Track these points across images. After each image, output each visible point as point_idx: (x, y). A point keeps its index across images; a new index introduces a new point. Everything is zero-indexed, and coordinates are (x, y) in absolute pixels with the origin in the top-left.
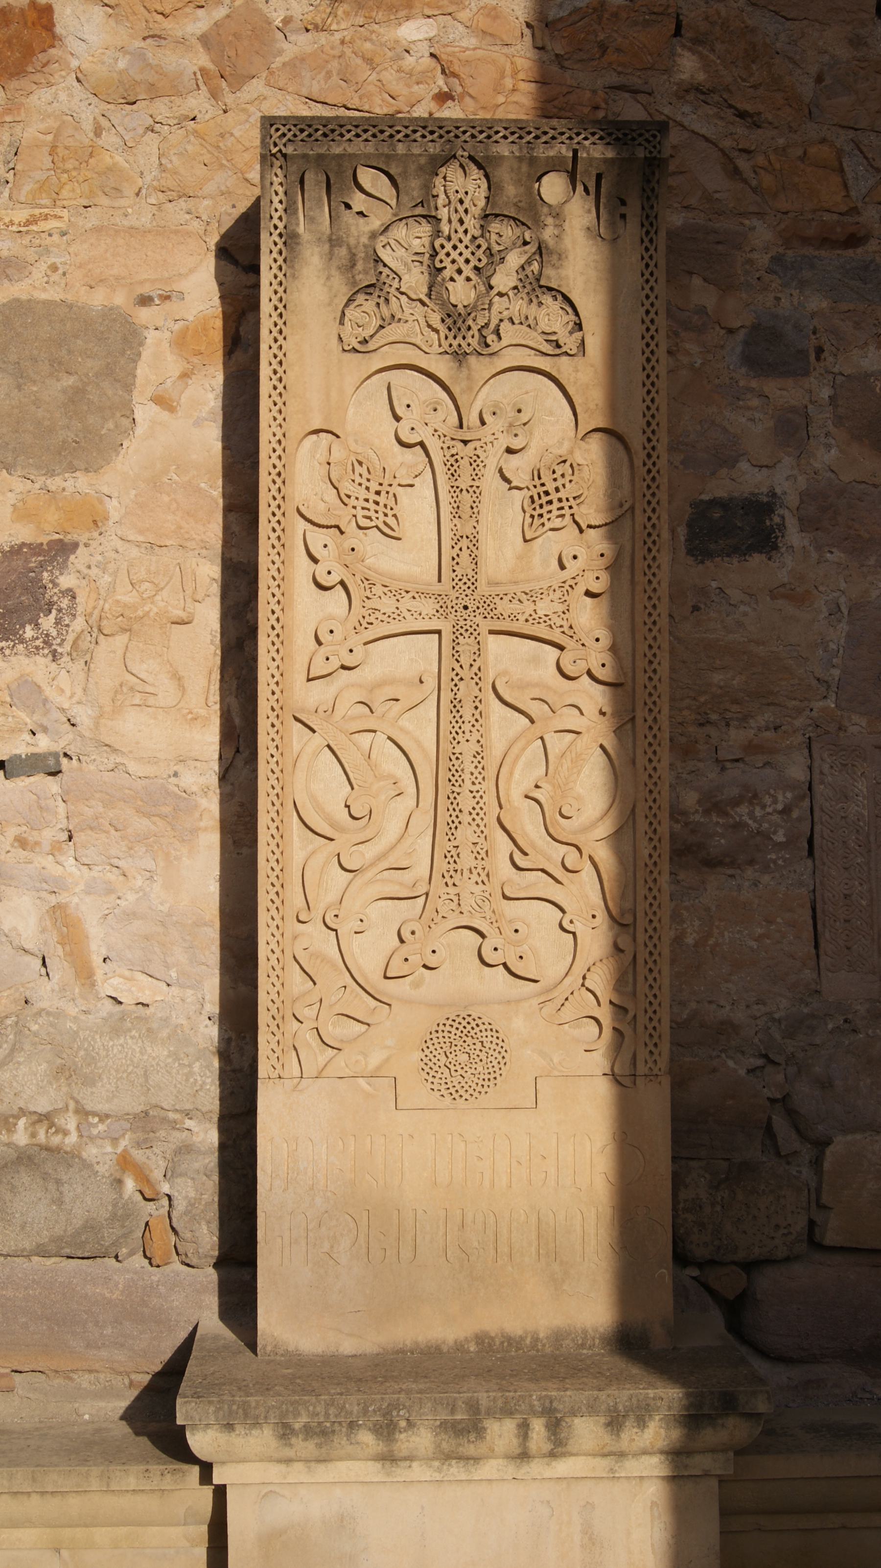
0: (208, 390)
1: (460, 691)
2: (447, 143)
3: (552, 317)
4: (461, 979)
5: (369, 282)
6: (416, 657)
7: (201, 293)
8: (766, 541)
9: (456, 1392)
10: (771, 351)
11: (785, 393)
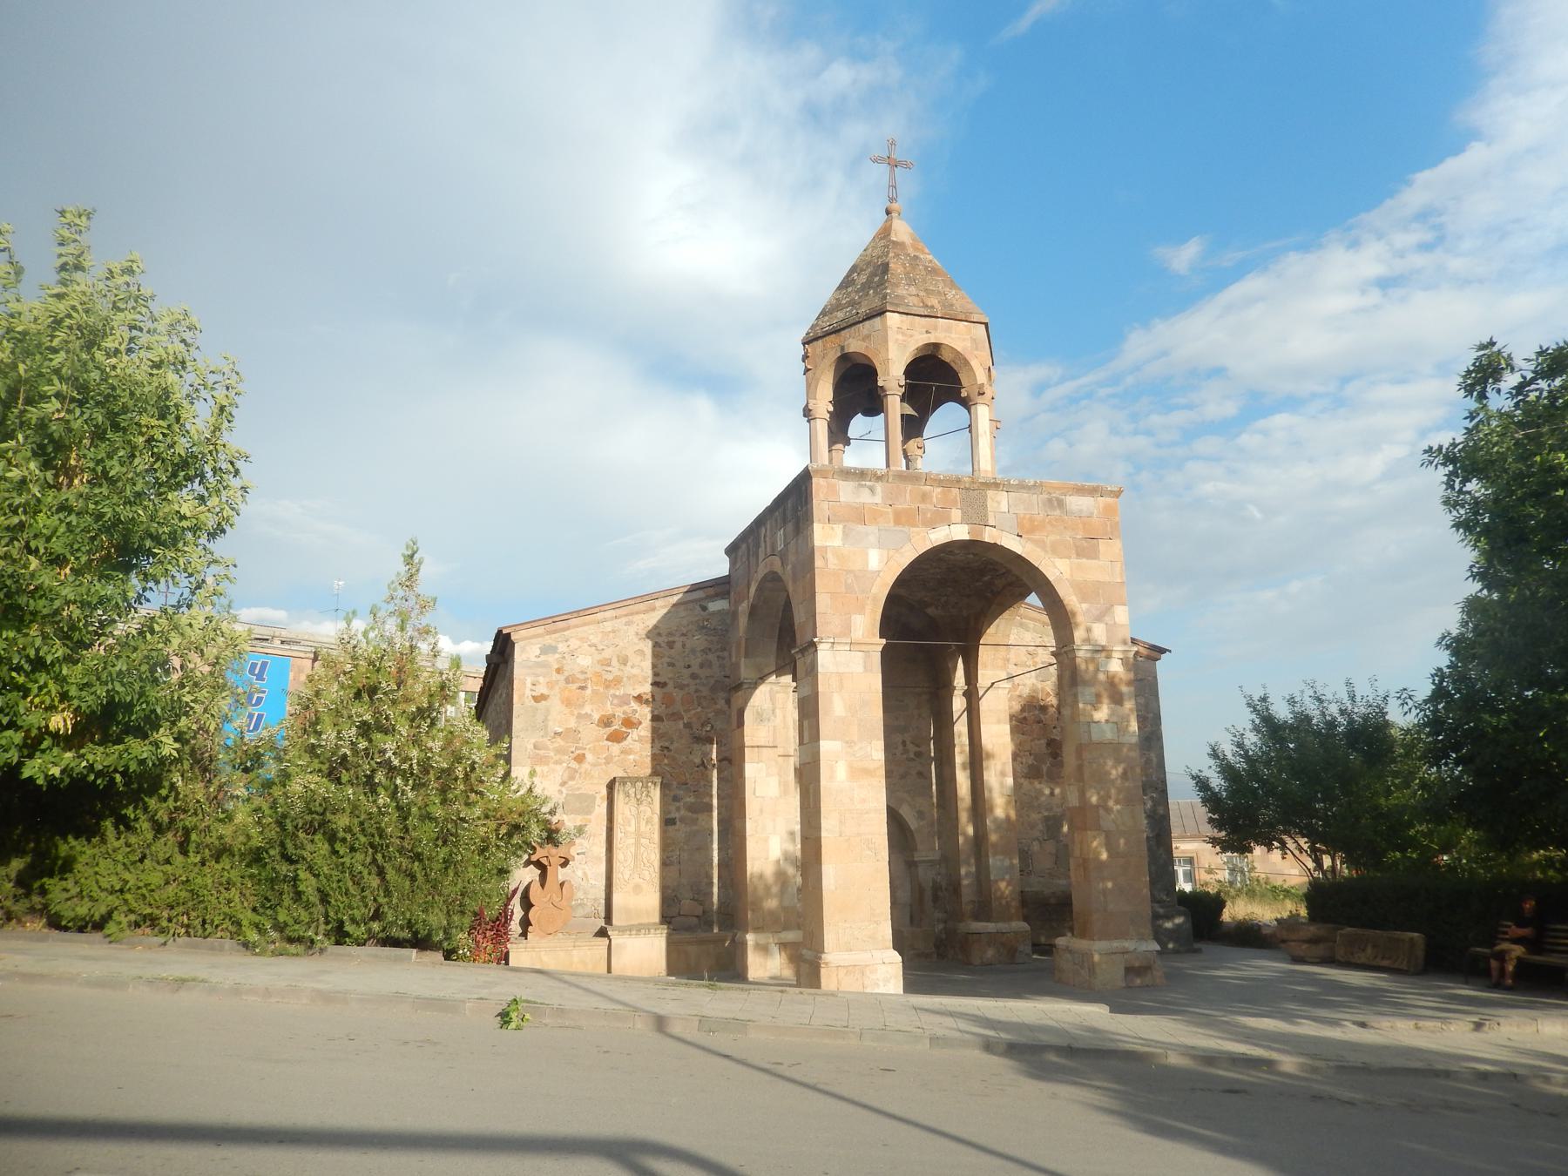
0: (605, 804)
1: (638, 844)
2: (638, 779)
4: (637, 880)
7: (604, 792)
9: (639, 929)
10: (676, 799)
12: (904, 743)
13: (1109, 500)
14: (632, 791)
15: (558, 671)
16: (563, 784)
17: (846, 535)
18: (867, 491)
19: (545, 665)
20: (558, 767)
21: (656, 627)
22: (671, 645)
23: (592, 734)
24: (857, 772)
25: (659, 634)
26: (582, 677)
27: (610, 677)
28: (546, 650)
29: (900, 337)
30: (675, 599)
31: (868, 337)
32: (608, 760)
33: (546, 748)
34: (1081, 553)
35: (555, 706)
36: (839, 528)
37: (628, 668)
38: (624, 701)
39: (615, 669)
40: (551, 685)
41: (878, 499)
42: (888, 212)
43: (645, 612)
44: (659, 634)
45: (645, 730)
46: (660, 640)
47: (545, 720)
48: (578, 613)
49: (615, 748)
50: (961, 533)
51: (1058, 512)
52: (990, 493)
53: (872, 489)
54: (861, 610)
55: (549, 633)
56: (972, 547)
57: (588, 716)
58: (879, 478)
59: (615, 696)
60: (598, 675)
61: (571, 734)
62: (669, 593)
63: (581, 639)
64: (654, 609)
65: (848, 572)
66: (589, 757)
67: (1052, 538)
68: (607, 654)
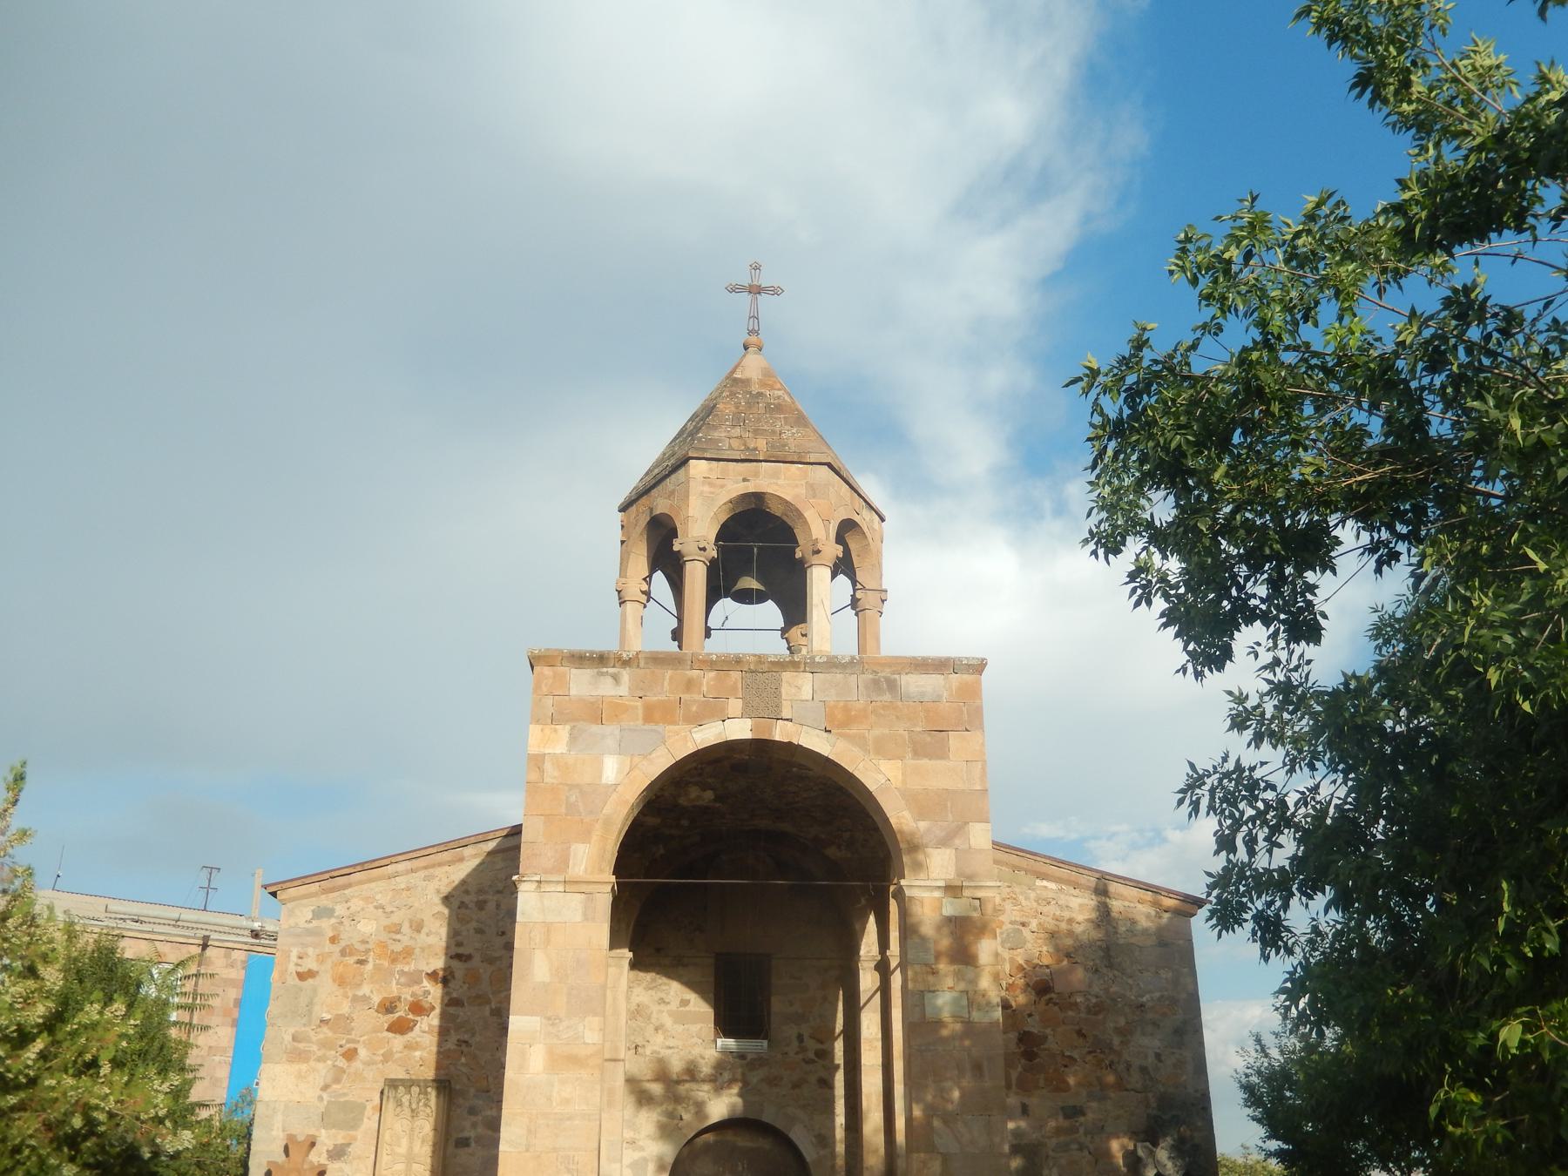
3: (428, 1110)
5: (399, 1104)
6: (400, 1167)
8: (468, 1145)
11: (473, 1119)
12: (800, 1038)
13: (967, 677)
14: (405, 1099)
15: (333, 940)
16: (325, 1088)
17: (573, 739)
18: (609, 680)
19: (316, 933)
20: (320, 1066)
21: (463, 882)
22: (481, 905)
23: (369, 1022)
24: (563, 1060)
25: (467, 892)
26: (362, 948)
27: (398, 948)
28: (320, 913)
29: (706, 488)
30: (491, 845)
31: (672, 492)
32: (387, 1057)
33: (307, 1040)
34: (919, 751)
35: (325, 986)
36: (564, 731)
37: (423, 936)
38: (414, 979)
39: (406, 939)
40: (321, 958)
41: (623, 690)
42: (746, 348)
43: (450, 863)
44: (467, 892)
45: (434, 1020)
46: (467, 899)
47: (310, 1004)
48: (364, 866)
49: (398, 1041)
50: (740, 729)
51: (887, 697)
52: (786, 676)
53: (616, 678)
54: (585, 836)
55: (325, 891)
56: (761, 747)
57: (365, 999)
58: (626, 663)
59: (402, 973)
60: (383, 945)
61: (340, 1023)
62: (482, 838)
63: (367, 899)
64: (461, 860)
65: (572, 787)
66: (363, 1053)
67: (877, 732)
68: (395, 919)
